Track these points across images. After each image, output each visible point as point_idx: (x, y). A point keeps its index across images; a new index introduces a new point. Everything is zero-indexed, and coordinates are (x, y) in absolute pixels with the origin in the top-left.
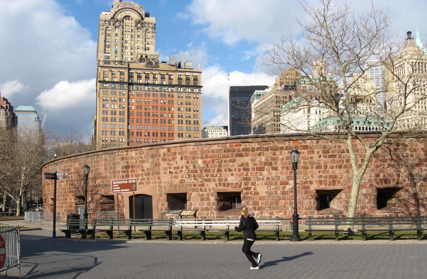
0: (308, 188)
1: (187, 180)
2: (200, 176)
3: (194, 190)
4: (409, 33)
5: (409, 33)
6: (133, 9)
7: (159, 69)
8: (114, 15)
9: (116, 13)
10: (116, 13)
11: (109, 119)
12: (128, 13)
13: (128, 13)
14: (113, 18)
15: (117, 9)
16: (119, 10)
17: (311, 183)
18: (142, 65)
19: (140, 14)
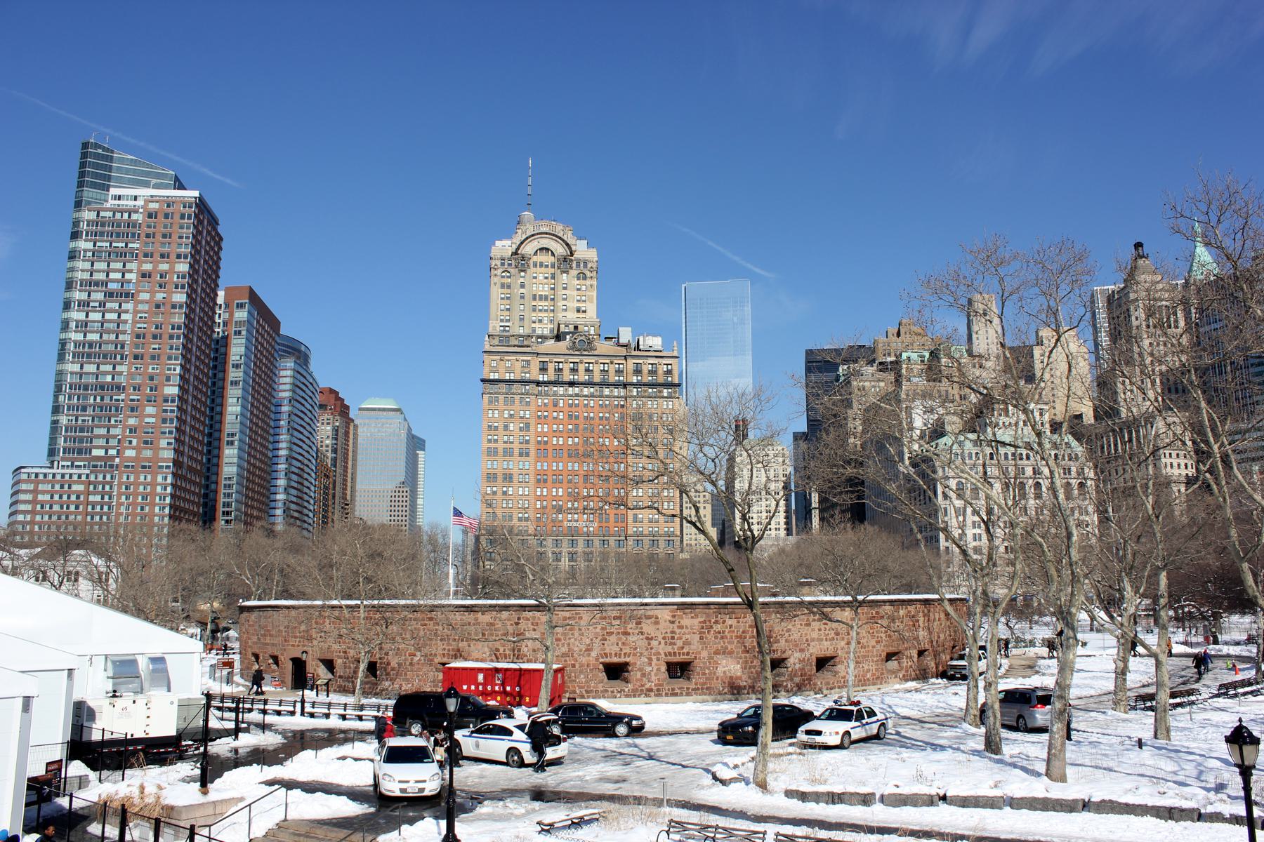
0: (432, 660)
1: (334, 646)
2: (344, 643)
3: (339, 657)
4: (1138, 245)
5: (1138, 245)
6: (554, 235)
7: (595, 353)
8: (518, 248)
9: (522, 243)
10: (522, 243)
11: (500, 450)
12: (545, 242)
13: (545, 242)
14: (515, 253)
15: (524, 237)
16: (527, 238)
17: (436, 655)
18: (562, 346)
19: (567, 244)
